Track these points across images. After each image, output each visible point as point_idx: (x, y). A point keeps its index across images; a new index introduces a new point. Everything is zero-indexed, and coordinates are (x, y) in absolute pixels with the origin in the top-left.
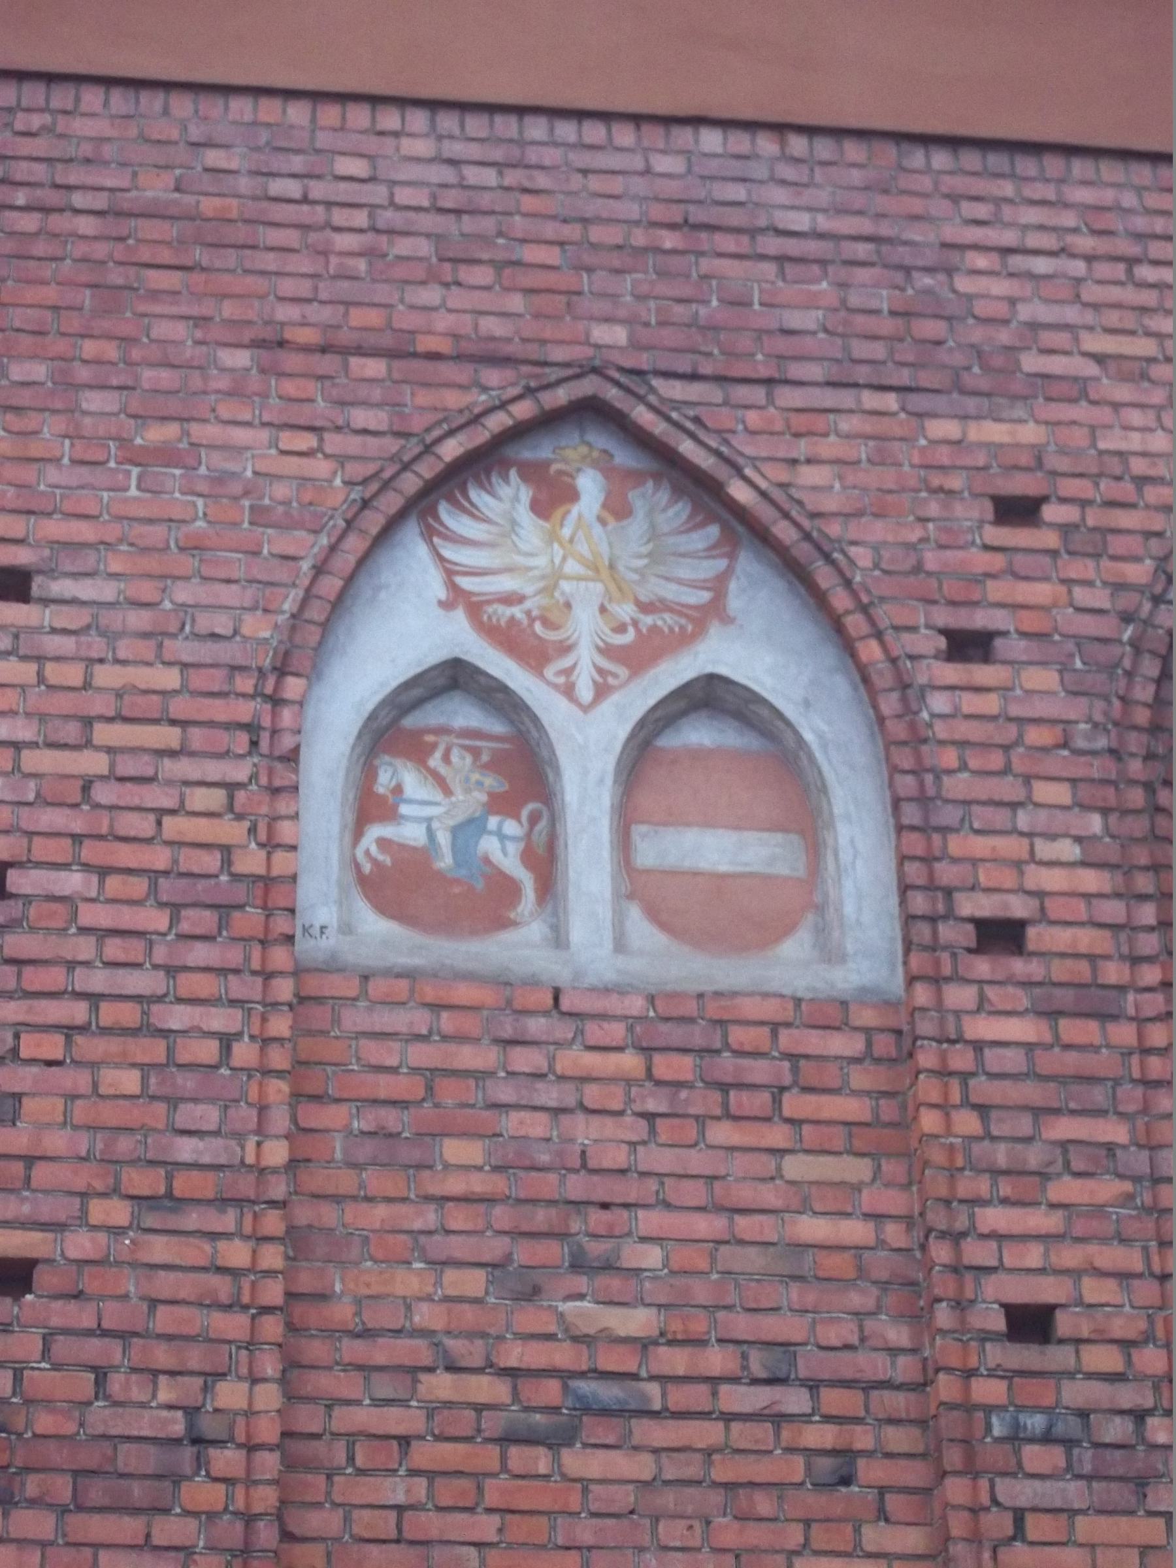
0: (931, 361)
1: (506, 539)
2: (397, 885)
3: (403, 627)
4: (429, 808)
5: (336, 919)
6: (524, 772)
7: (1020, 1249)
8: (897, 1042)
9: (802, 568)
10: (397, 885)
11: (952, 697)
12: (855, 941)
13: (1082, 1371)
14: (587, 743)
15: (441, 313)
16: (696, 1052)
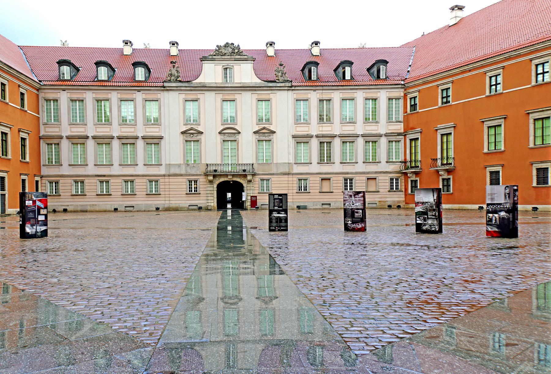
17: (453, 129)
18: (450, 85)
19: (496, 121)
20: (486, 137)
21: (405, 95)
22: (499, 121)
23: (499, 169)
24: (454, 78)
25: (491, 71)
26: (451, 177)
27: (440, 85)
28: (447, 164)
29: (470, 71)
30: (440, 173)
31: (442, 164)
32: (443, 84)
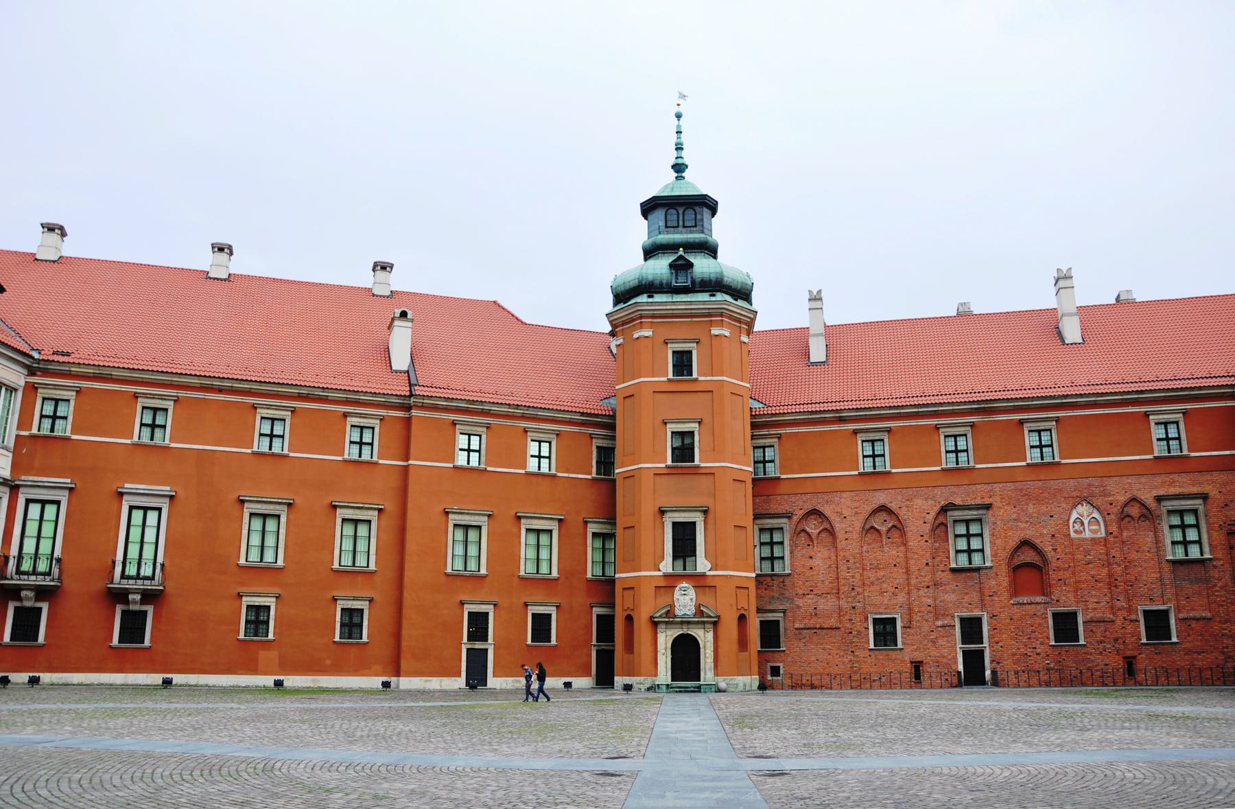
0: (1105, 494)
1: (1083, 509)
2: (1076, 532)
3: (1074, 516)
4: (1077, 527)
5: (1073, 535)
6: (1082, 524)
7: (1113, 552)
8: (1105, 539)
9: (1098, 509)
10: (1076, 532)
11: (1108, 518)
12: (1102, 534)
13: (1117, 560)
14: (1086, 522)
15: (1074, 494)
16: (1094, 541)
17: (167, 500)
18: (170, 405)
19: (272, 507)
20: (245, 532)
21: (31, 389)
22: (278, 507)
23: (270, 601)
24: (182, 394)
25: (269, 407)
26: (150, 609)
27: (146, 396)
28: (138, 577)
29: (220, 390)
30: (131, 597)
31: (123, 576)
32: (153, 397)
